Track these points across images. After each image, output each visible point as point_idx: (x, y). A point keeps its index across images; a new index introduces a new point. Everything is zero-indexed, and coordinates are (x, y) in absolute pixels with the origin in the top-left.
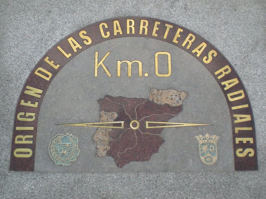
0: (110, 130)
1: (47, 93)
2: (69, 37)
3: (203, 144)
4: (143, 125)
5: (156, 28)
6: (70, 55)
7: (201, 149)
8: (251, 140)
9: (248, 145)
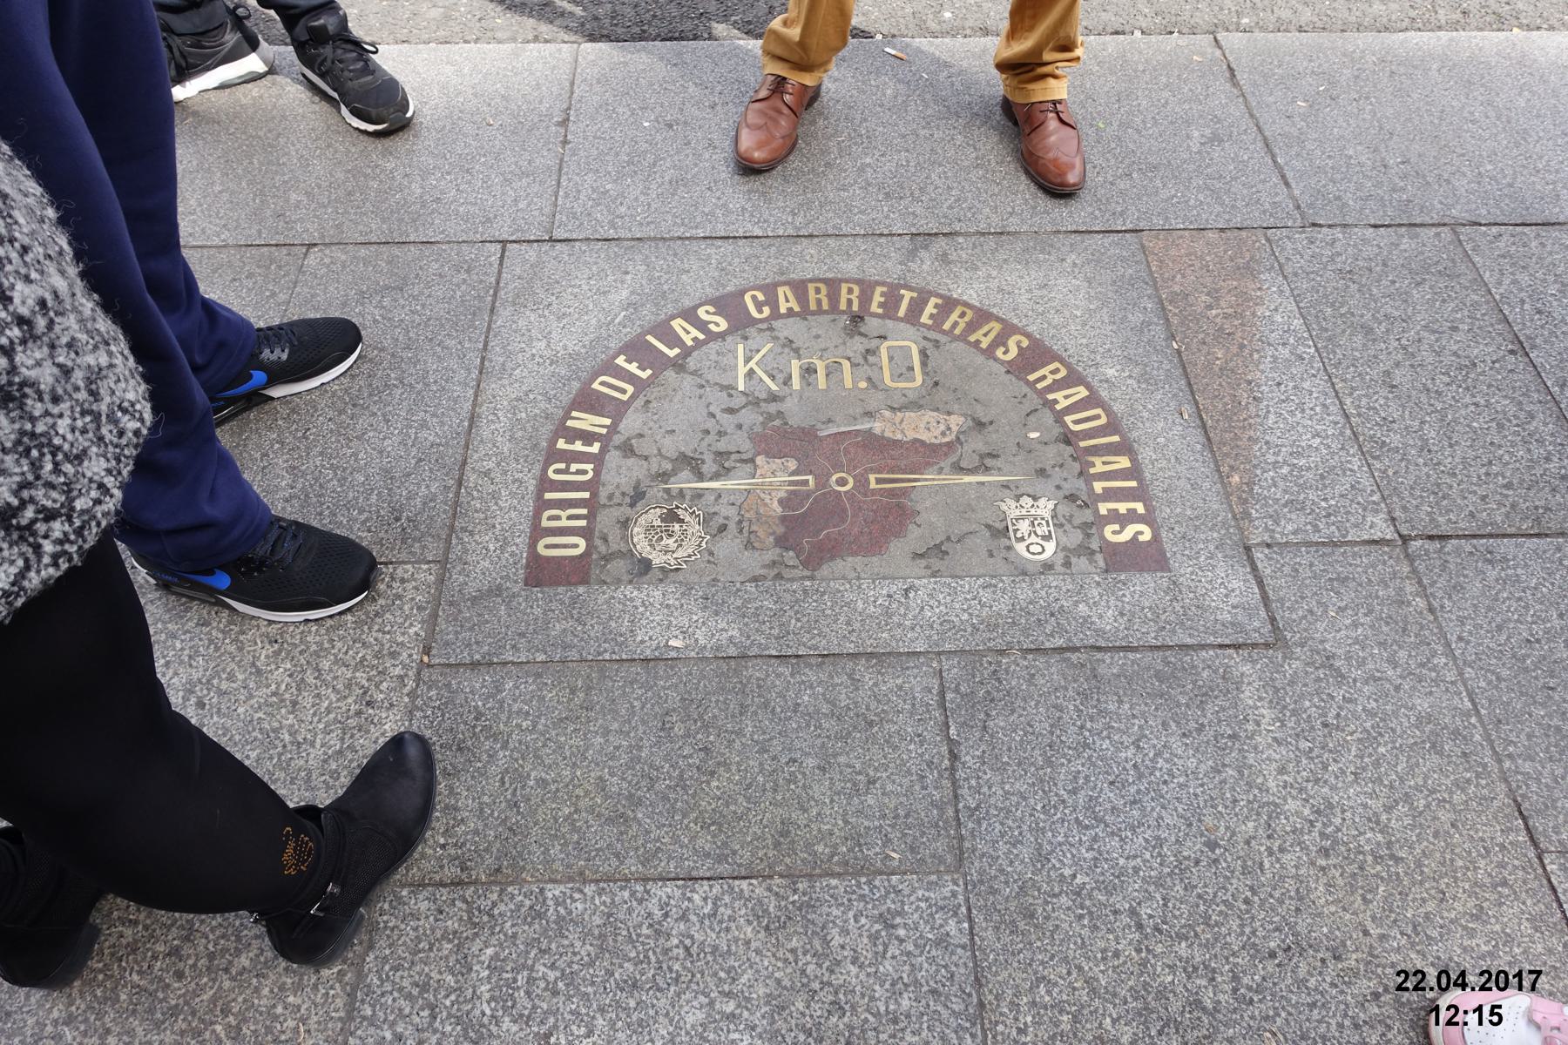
2: (673, 317)
4: (862, 482)
6: (677, 351)
8: (1140, 508)
9: (1133, 516)
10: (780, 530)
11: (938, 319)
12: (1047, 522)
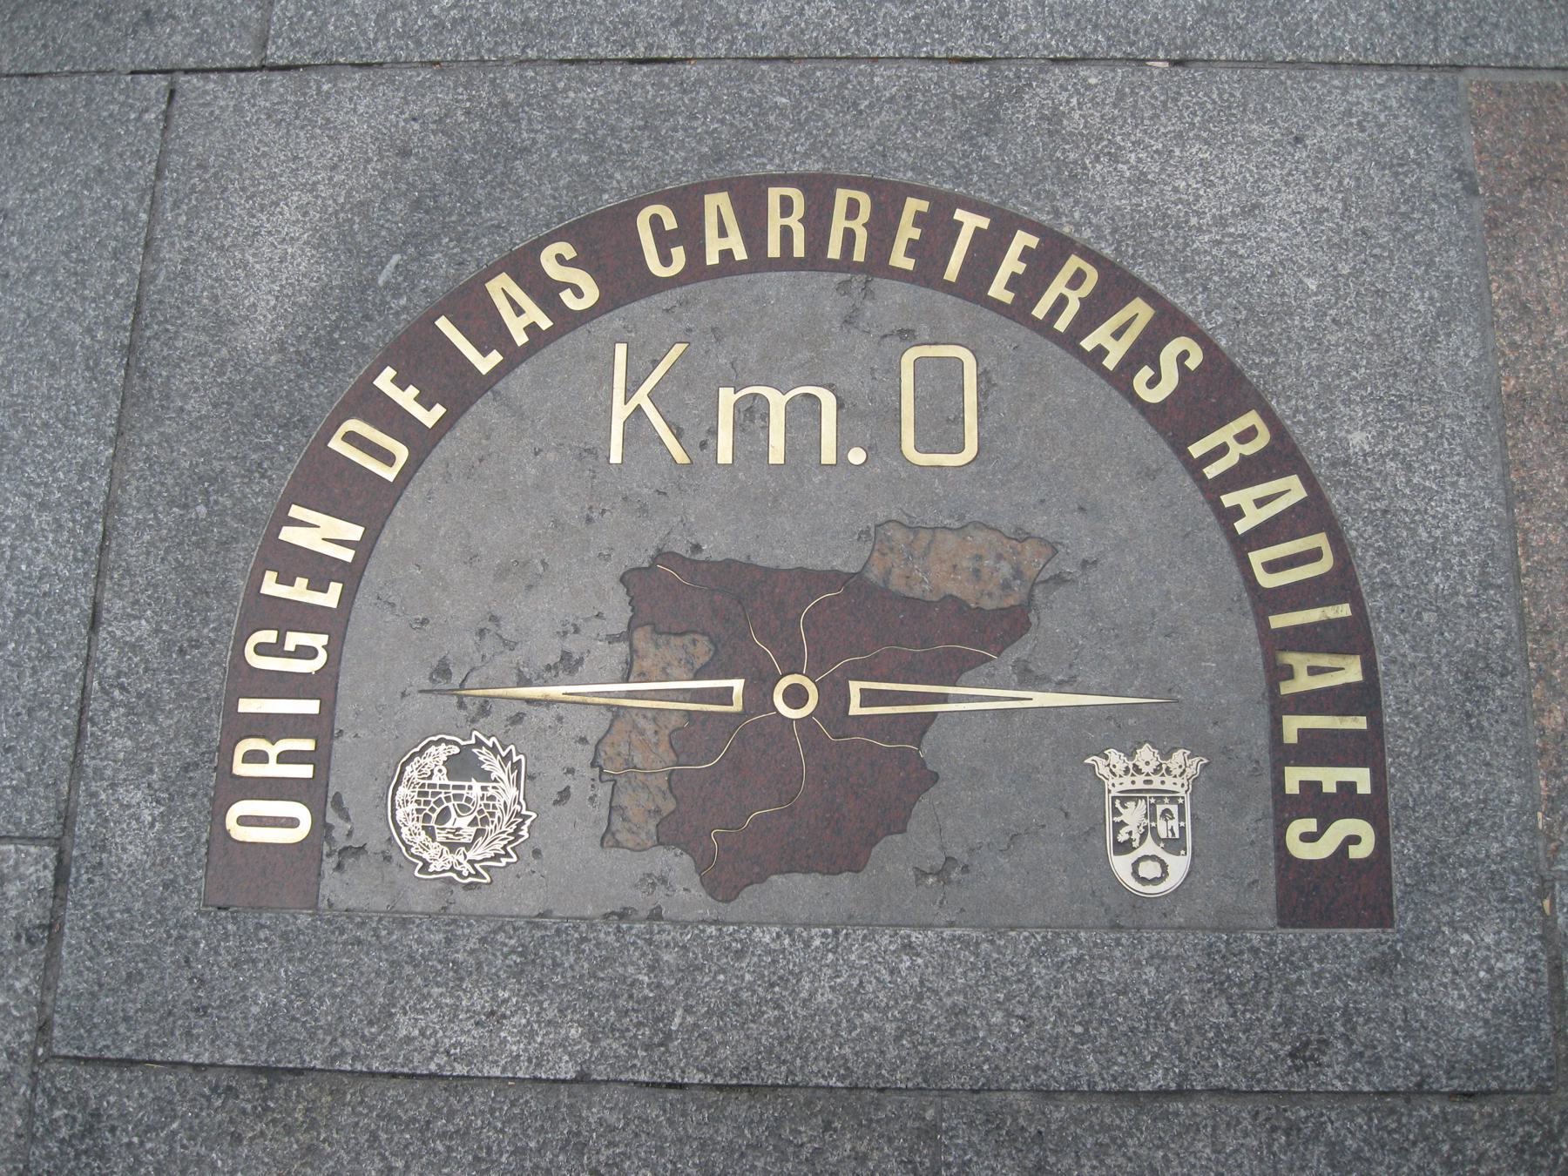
0: (675, 722)
1: (384, 541)
2: (492, 273)
3: (1126, 798)
4: (835, 696)
5: (907, 231)
7: (1117, 819)
8: (1362, 779)
9: (1345, 802)
10: (669, 805)
12: (1181, 807)
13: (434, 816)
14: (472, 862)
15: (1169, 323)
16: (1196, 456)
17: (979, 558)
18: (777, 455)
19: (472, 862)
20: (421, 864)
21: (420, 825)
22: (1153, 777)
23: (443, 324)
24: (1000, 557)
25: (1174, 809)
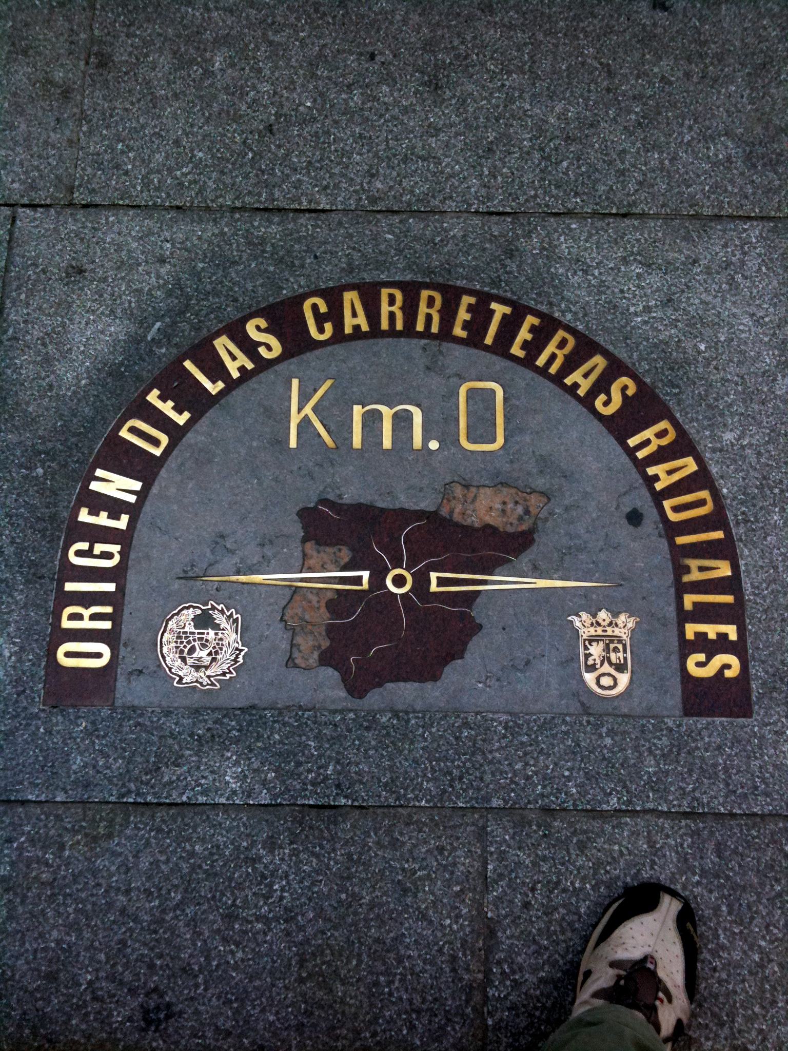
0: (330, 595)
1: (155, 490)
2: (218, 334)
3: (592, 640)
4: (421, 581)
6: (220, 385)
7: (587, 652)
8: (731, 631)
9: (722, 644)
10: (326, 644)
11: (534, 348)
13: (186, 650)
14: (209, 677)
15: (616, 368)
16: (631, 446)
17: (504, 503)
18: (387, 443)
19: (209, 677)
20: (178, 678)
21: (177, 655)
22: (607, 628)
23: (188, 364)
24: (516, 503)
25: (620, 647)
